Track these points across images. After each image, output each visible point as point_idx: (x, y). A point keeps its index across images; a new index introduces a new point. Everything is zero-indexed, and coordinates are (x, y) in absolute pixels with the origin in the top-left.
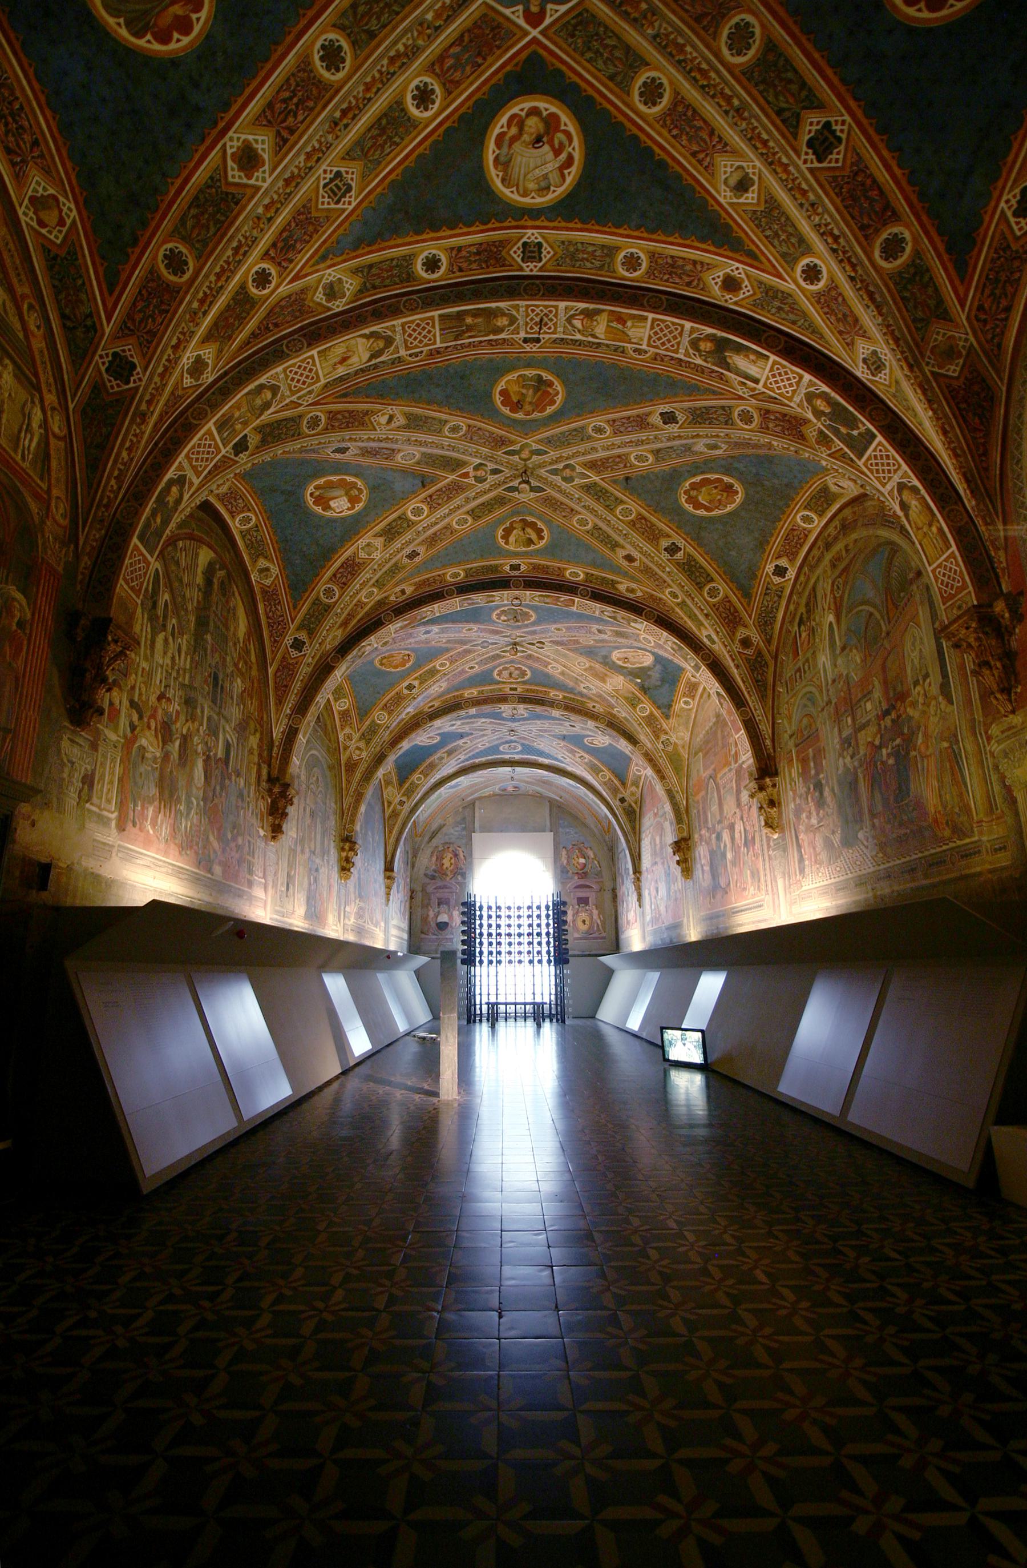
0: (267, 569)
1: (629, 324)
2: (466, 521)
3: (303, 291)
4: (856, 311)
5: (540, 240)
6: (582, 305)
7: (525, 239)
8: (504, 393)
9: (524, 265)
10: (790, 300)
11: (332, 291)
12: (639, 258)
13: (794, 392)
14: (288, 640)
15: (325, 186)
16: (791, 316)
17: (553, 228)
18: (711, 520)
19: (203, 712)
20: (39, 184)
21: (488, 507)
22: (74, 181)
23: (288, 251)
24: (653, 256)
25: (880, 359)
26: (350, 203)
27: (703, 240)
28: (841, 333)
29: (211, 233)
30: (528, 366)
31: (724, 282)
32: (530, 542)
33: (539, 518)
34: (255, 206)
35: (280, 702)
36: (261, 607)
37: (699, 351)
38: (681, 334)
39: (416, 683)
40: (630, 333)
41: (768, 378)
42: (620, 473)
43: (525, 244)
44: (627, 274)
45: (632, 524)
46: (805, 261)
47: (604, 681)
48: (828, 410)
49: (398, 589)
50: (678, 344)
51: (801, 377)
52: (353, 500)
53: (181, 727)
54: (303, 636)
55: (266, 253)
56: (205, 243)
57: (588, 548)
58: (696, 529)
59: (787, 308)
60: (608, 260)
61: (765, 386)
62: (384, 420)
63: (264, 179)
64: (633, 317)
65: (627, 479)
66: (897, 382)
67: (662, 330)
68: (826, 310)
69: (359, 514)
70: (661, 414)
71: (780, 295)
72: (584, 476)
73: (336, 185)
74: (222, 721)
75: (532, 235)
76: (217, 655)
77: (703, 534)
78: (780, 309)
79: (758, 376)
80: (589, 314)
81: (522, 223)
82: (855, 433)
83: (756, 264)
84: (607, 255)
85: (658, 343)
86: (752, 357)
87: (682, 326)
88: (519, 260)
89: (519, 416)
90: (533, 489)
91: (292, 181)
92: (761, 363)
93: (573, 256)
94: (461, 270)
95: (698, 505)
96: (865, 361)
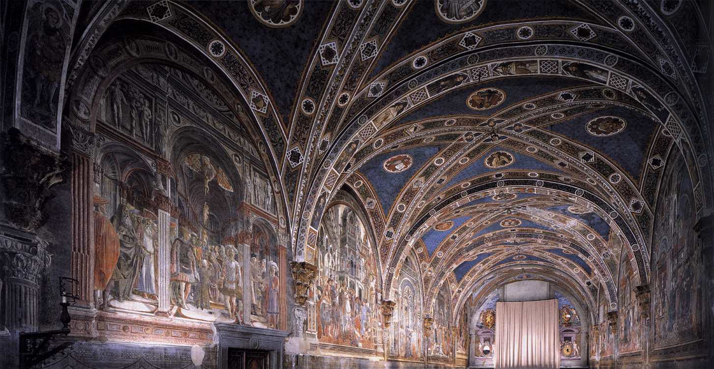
0: (371, 202)
2: (466, 160)
3: (363, 95)
5: (473, 35)
7: (465, 37)
8: (472, 102)
9: (468, 48)
11: (375, 91)
14: (385, 233)
15: (363, 52)
18: (610, 138)
19: (347, 281)
20: (254, 93)
21: (477, 151)
22: (266, 87)
23: (352, 84)
26: (376, 54)
29: (320, 89)
30: (482, 88)
32: (504, 162)
33: (507, 151)
34: (336, 72)
35: (384, 262)
36: (371, 219)
39: (457, 235)
42: (547, 123)
43: (465, 39)
45: (560, 147)
47: (564, 222)
49: (436, 198)
52: (406, 164)
53: (338, 290)
54: (391, 230)
55: (344, 88)
56: (318, 95)
57: (538, 162)
58: (600, 145)
60: (512, 35)
62: (412, 130)
63: (337, 60)
65: (552, 126)
69: (410, 169)
70: (562, 95)
72: (527, 128)
73: (368, 49)
74: (357, 281)
75: (468, 34)
76: (351, 253)
77: (605, 146)
81: (462, 30)
88: (464, 46)
89: (484, 108)
90: (500, 138)
91: (349, 57)
94: (435, 59)
95: (599, 132)
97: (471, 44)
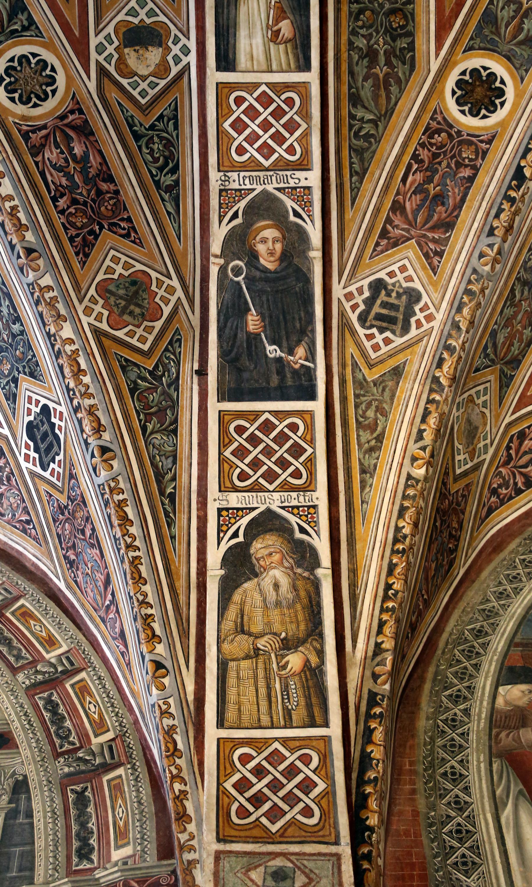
4: (465, 215)
10: (401, 71)
13: (253, 165)
16: (366, 91)
25: (409, 313)
28: (397, 207)
46: (499, 68)
48: (268, 263)
51: (303, 165)
61: (223, 89)
66: (397, 373)
68: (424, 154)
71: (402, 43)
78: (371, 55)
79: (242, 60)
82: (272, 351)
86: (286, 27)
96: (378, 286)
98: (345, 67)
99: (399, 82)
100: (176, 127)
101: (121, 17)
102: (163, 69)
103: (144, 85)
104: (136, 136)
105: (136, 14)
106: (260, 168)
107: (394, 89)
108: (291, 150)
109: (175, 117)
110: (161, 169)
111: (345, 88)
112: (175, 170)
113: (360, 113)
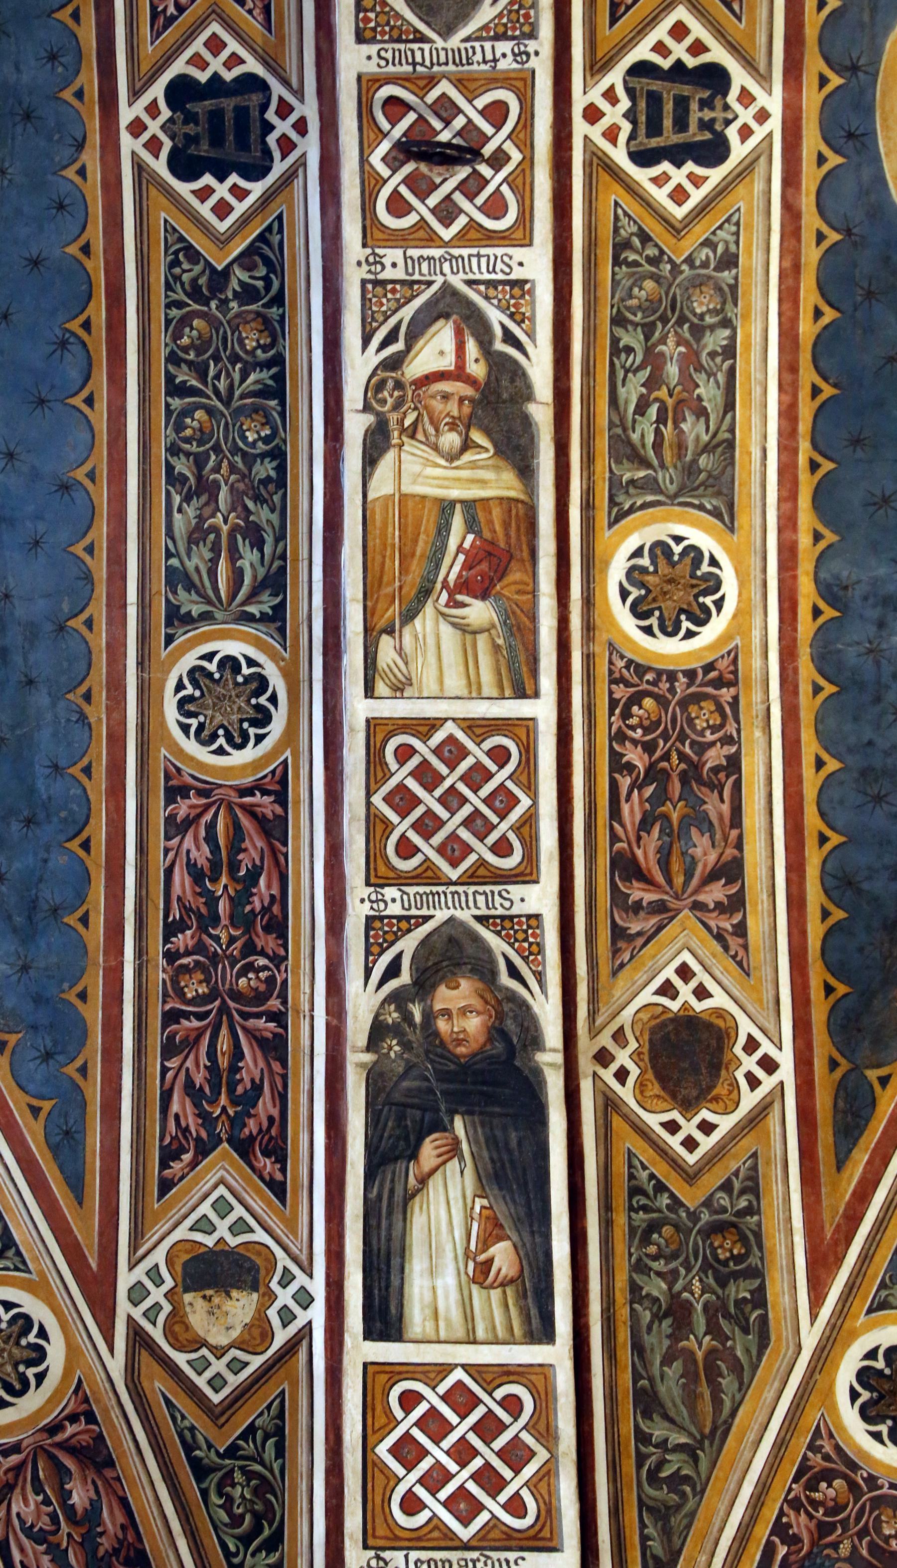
1: (479, 612)
5: (739, 151)
6: (539, 368)
7: (739, 77)
9: (615, 77)
10: (740, 1345)
12: (702, 618)
16: (670, 1384)
17: (791, 211)
24: (720, 677)
27: (841, 883)
31: (688, 1022)
37: (424, 985)
38: (481, 875)
40: (426, 621)
41: (434, 1373)
43: (716, 78)
44: (616, 572)
50: (427, 875)
59: (699, 1344)
60: (668, 479)
64: (519, 627)
67: (476, 777)
71: (741, 1290)
78: (677, 1312)
79: (416, 1318)
80: (496, 408)
81: (814, 63)
83: (825, 1136)
84: (691, 470)
85: (401, 775)
87: (527, 874)
92: (491, 1306)
93: (668, 312)
97: (648, 114)
98: (624, 1335)
99: (737, 1368)
100: (280, 1451)
101: (181, 1233)
102: (258, 1333)
103: (219, 1366)
104: (195, 1468)
105: (211, 1229)
106: (450, 1542)
107: (727, 1382)
108: (515, 1506)
109: (279, 1431)
110: (246, 1540)
111: (626, 1379)
112: (274, 1542)
113: (658, 1431)
